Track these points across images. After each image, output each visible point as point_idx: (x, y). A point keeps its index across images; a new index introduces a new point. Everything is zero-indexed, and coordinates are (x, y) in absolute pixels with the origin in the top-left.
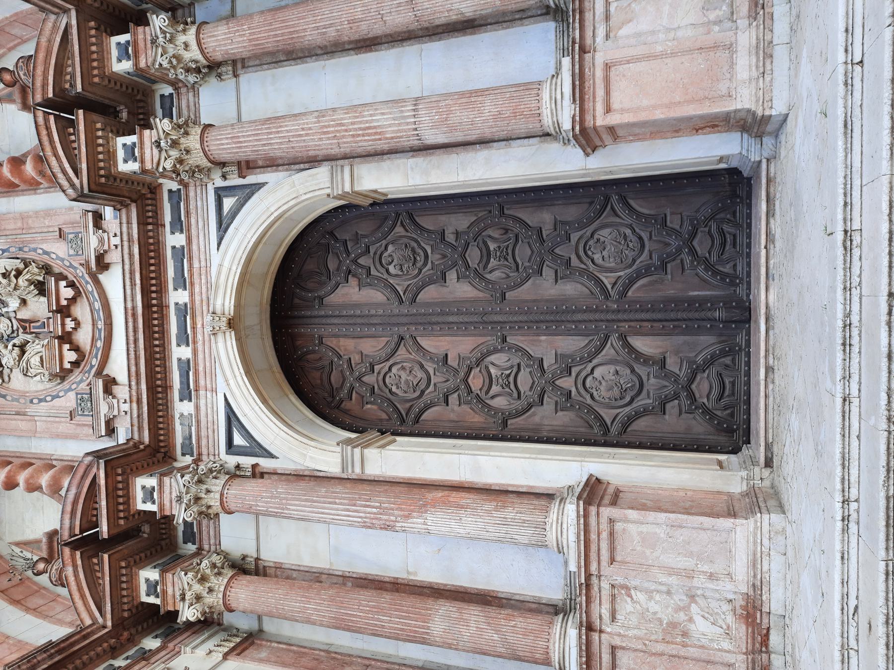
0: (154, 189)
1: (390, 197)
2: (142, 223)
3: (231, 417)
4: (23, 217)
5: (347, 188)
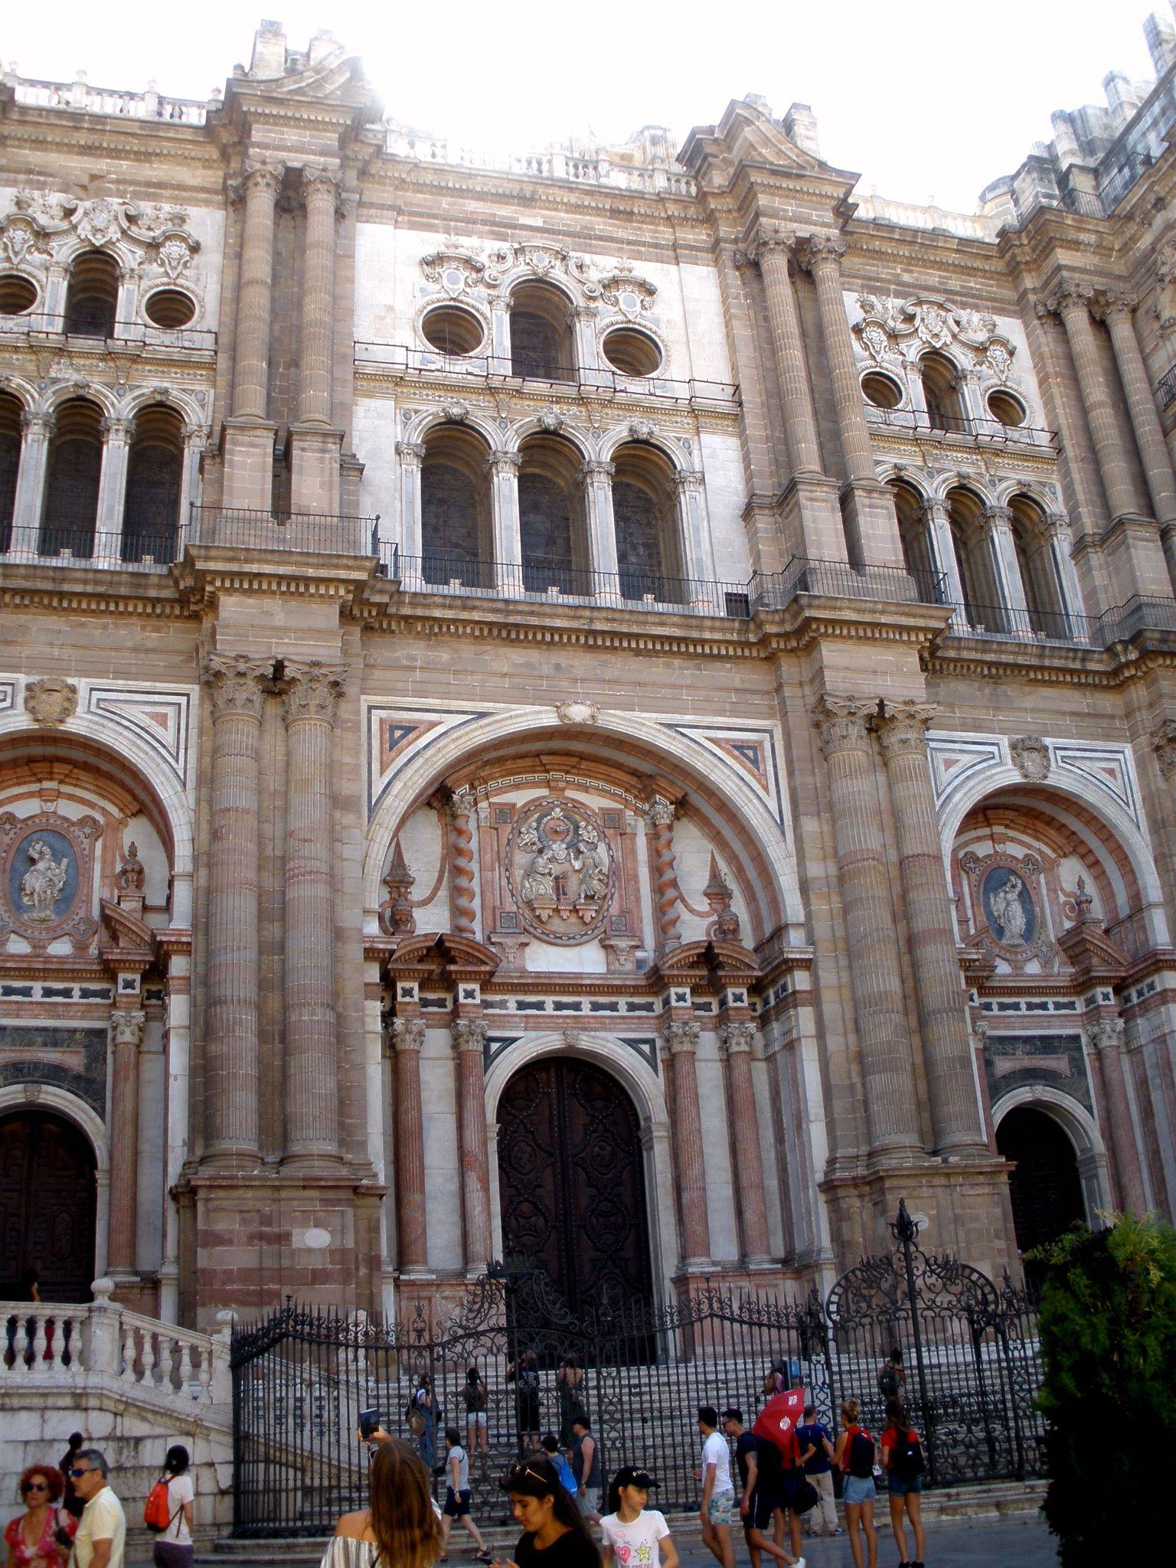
0: (656, 994)
1: (645, 1154)
2: (634, 987)
3: (508, 1042)
4: (636, 877)
5: (655, 1134)
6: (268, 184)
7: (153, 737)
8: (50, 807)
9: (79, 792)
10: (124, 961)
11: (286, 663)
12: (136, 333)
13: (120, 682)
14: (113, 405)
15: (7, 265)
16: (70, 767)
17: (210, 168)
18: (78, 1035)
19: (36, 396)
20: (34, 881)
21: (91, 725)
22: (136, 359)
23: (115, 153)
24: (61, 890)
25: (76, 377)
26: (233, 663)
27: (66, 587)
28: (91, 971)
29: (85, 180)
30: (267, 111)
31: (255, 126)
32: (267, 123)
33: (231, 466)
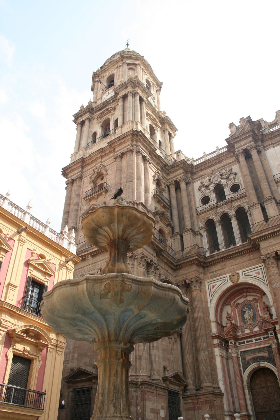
6: (241, 155)
7: (258, 278)
8: (246, 299)
9: (251, 294)
10: (268, 329)
11: (278, 252)
12: (230, 196)
13: (248, 268)
14: (230, 212)
15: (203, 195)
16: (247, 289)
17: (233, 157)
18: (265, 348)
19: (215, 217)
20: (246, 316)
21: (244, 280)
22: (232, 201)
23: (215, 164)
24: (253, 316)
25: (222, 210)
26: (266, 256)
27: (230, 253)
28: (264, 333)
29: (212, 172)
30: (236, 141)
31: (235, 145)
32: (237, 143)
33: (253, 215)
